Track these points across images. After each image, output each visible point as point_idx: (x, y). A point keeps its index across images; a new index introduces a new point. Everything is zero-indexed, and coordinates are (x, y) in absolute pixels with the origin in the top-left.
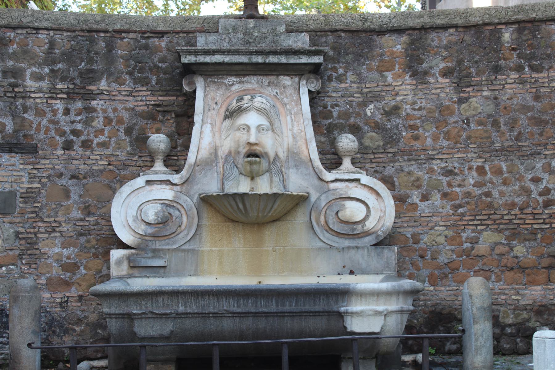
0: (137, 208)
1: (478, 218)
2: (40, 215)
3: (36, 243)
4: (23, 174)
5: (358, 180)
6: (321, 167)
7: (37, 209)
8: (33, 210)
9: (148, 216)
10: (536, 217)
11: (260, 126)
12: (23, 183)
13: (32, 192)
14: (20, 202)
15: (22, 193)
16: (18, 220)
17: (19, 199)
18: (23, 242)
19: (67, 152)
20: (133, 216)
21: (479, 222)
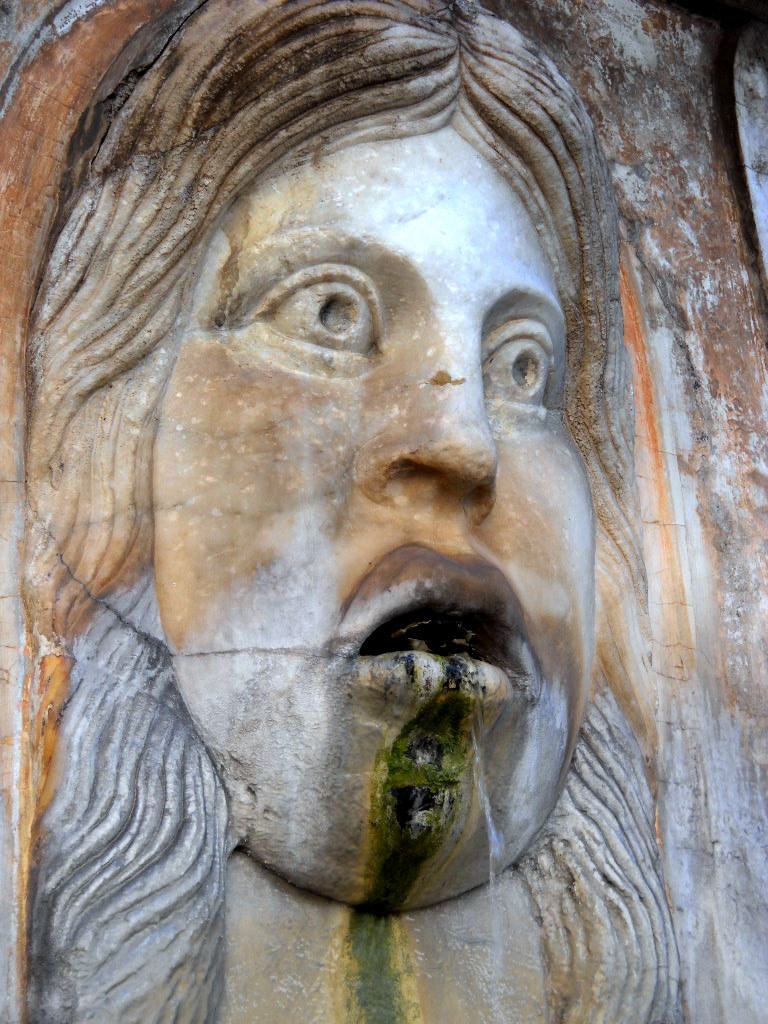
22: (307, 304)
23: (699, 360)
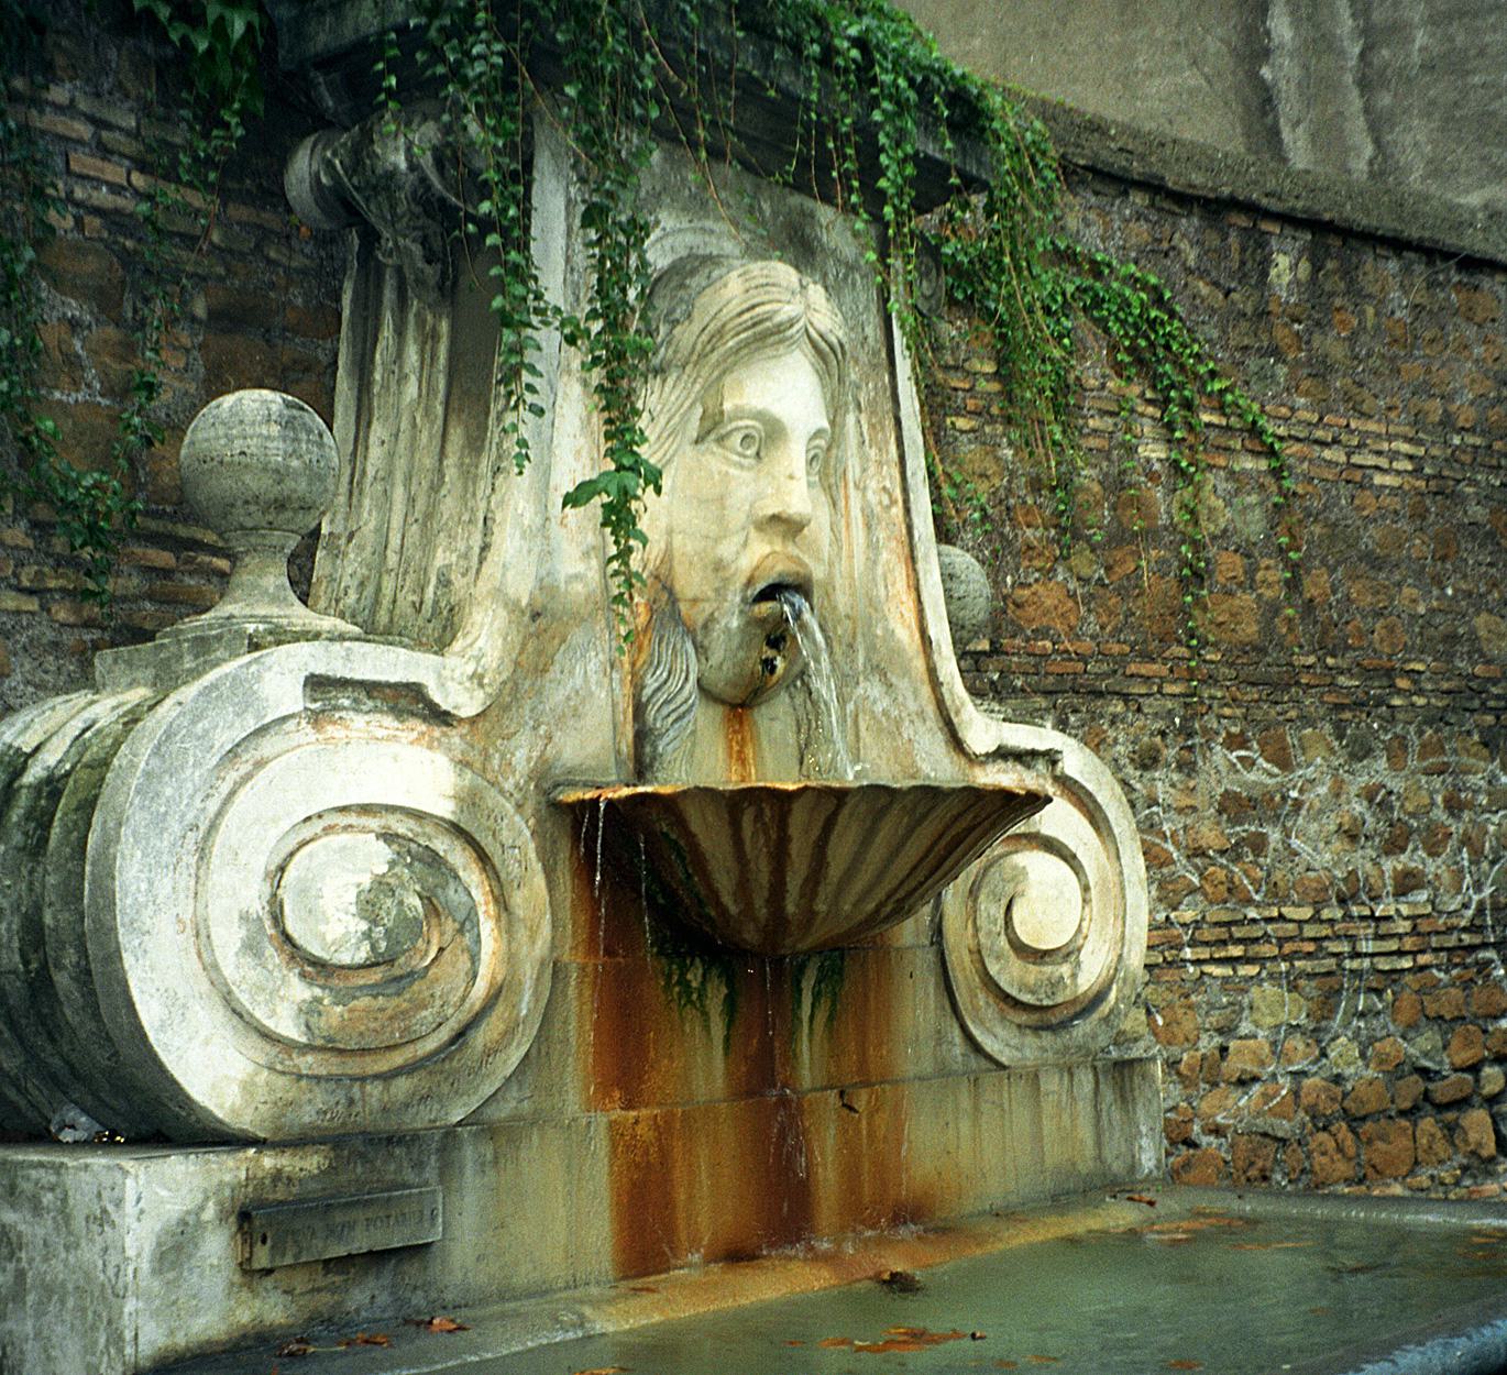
1: (1238, 932)
10: (1384, 928)
20: (244, 918)
21: (1236, 951)
22: (737, 438)
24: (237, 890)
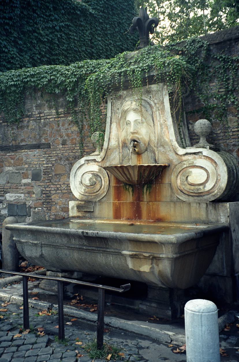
0: (81, 177)
2: (52, 181)
3: (50, 196)
4: (44, 159)
5: (201, 152)
6: (177, 145)
7: (50, 178)
8: (49, 178)
9: (85, 181)
11: (136, 121)
12: (44, 164)
13: (48, 169)
14: (43, 175)
15: (44, 170)
16: (41, 184)
17: (42, 173)
18: (44, 195)
19: (64, 146)
23: (160, 113)
24: (78, 179)
